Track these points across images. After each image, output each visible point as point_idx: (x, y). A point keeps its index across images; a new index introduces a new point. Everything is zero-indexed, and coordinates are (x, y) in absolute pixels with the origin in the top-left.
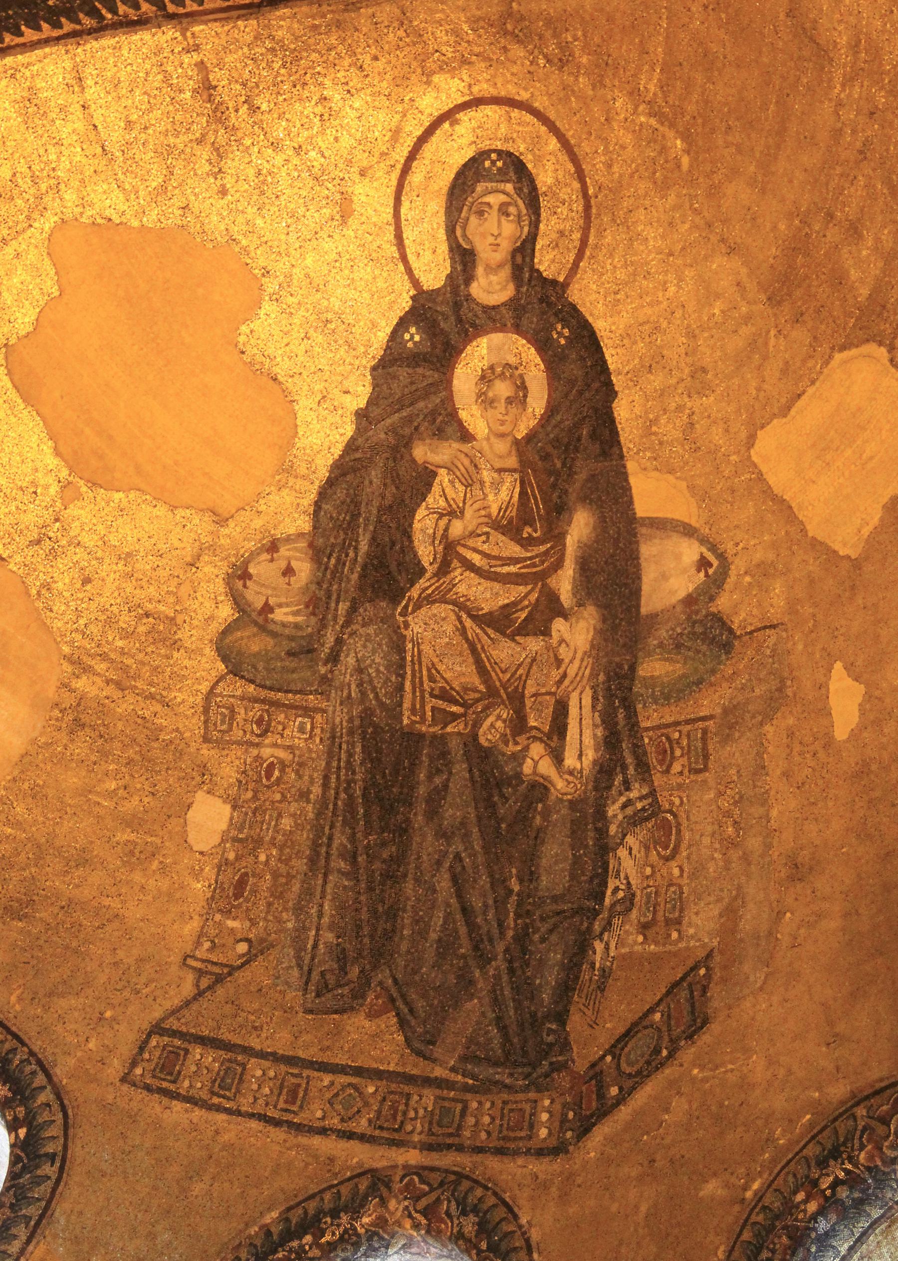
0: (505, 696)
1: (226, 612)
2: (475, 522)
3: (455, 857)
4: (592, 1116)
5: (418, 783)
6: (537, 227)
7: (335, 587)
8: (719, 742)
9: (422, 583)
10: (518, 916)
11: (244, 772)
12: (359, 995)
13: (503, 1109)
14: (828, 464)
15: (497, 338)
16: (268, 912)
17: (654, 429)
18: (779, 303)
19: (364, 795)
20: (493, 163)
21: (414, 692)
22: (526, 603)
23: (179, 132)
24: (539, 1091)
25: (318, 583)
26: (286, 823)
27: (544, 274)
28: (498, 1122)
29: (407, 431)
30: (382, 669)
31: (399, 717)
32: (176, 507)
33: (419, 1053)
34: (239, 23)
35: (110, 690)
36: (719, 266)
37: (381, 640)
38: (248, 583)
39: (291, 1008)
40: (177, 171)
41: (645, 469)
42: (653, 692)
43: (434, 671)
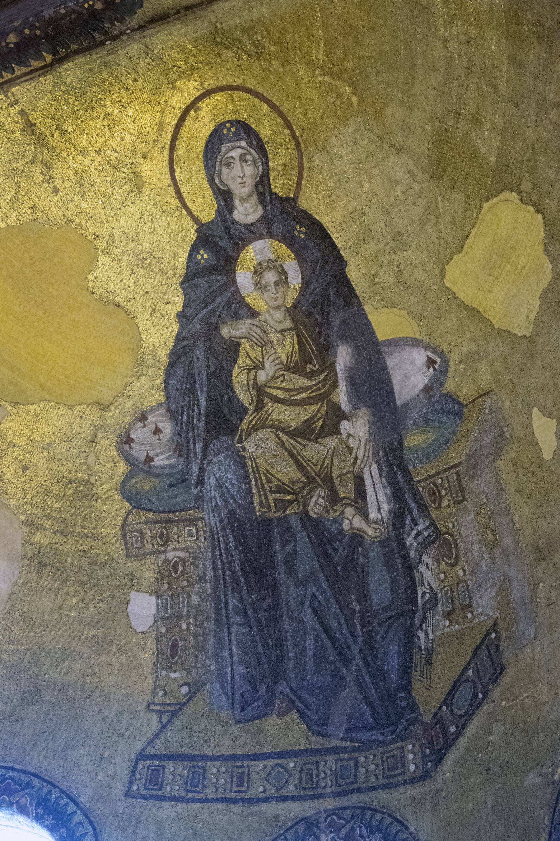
1: (122, 468)
2: (273, 370)
3: (312, 597)
4: (442, 749)
5: (276, 552)
6: (268, 166)
7: (190, 434)
8: (469, 479)
9: (248, 418)
10: (363, 626)
11: (159, 572)
12: (269, 703)
13: (382, 758)
15: (258, 244)
16: (196, 662)
17: (377, 280)
18: (439, 178)
19: (242, 569)
20: (229, 129)
21: (259, 492)
23: (18, 159)
24: (403, 740)
25: (179, 434)
26: (195, 599)
27: (280, 195)
28: (380, 767)
29: (214, 319)
31: (253, 511)
32: (73, 406)
33: (319, 734)
34: (41, 79)
35: (59, 538)
36: (393, 163)
37: (229, 462)
39: (226, 722)
40: (22, 185)
41: (377, 308)
42: (418, 455)
43: (269, 475)
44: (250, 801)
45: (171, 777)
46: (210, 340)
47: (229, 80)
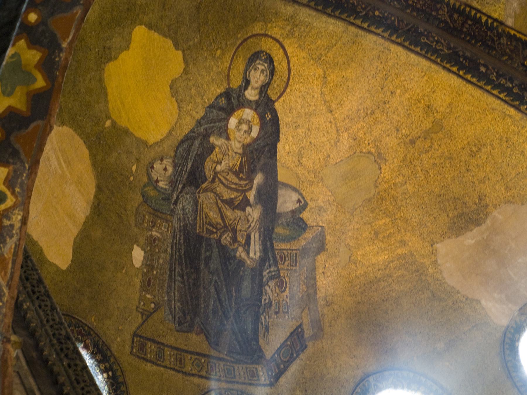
0: (230, 229)
1: (145, 179)
6: (271, 81)
10: (235, 304)
12: (191, 326)
14: (346, 184)
16: (158, 293)
19: (184, 254)
21: (200, 221)
22: (238, 199)
24: (257, 364)
25: (174, 176)
26: (161, 261)
28: (246, 374)
29: (210, 131)
30: (190, 211)
42: (279, 238)
45: (149, 350)
46: (204, 139)
47: (278, 37)
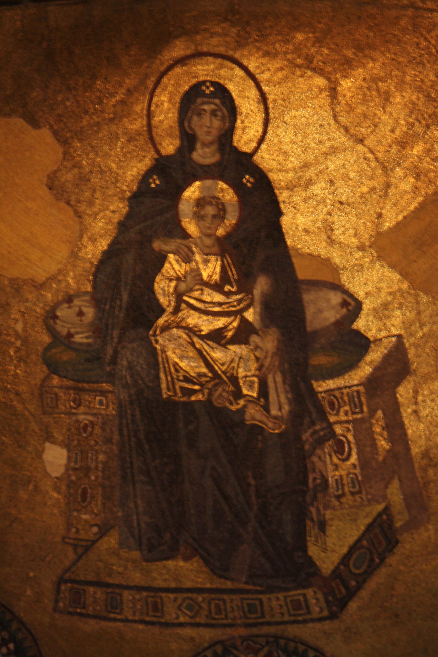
0: (225, 379)
1: (46, 339)
7: (110, 321)
15: (208, 182)
22: (231, 327)
24: (304, 587)
25: (100, 320)
30: (144, 366)
33: (221, 577)
38: (58, 321)
44: (166, 625)
45: (92, 599)
47: (222, 50)
